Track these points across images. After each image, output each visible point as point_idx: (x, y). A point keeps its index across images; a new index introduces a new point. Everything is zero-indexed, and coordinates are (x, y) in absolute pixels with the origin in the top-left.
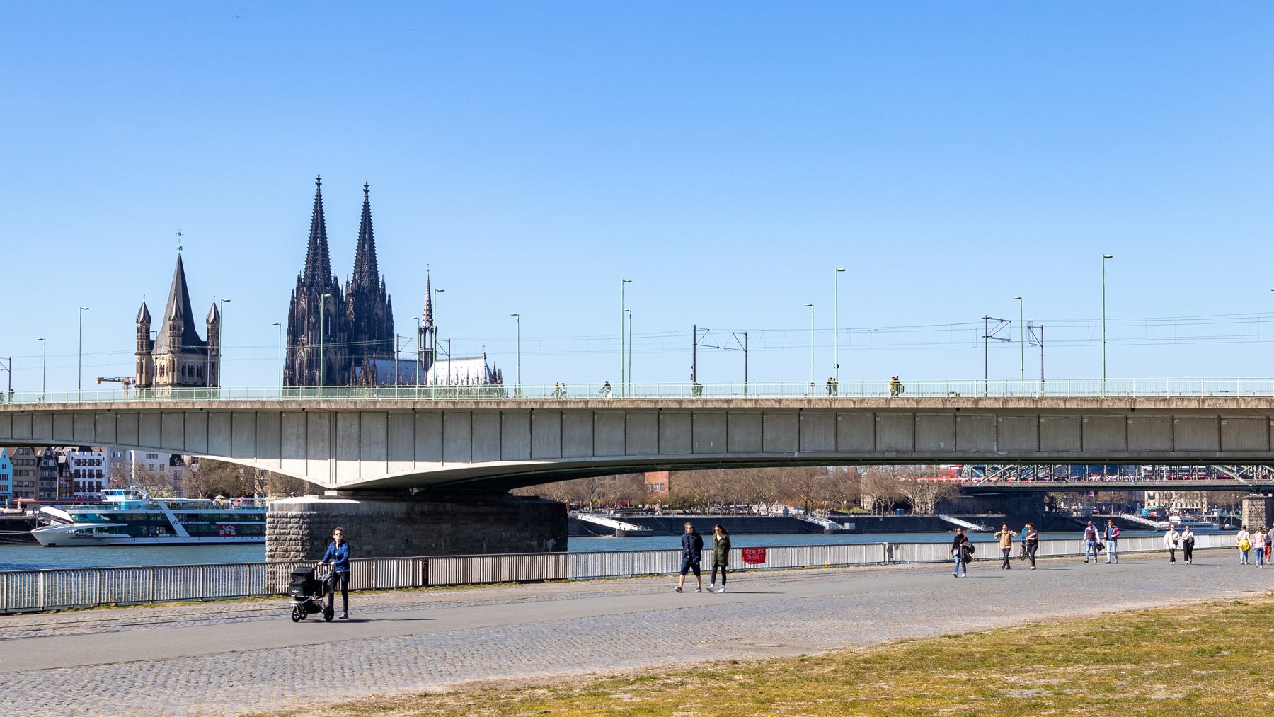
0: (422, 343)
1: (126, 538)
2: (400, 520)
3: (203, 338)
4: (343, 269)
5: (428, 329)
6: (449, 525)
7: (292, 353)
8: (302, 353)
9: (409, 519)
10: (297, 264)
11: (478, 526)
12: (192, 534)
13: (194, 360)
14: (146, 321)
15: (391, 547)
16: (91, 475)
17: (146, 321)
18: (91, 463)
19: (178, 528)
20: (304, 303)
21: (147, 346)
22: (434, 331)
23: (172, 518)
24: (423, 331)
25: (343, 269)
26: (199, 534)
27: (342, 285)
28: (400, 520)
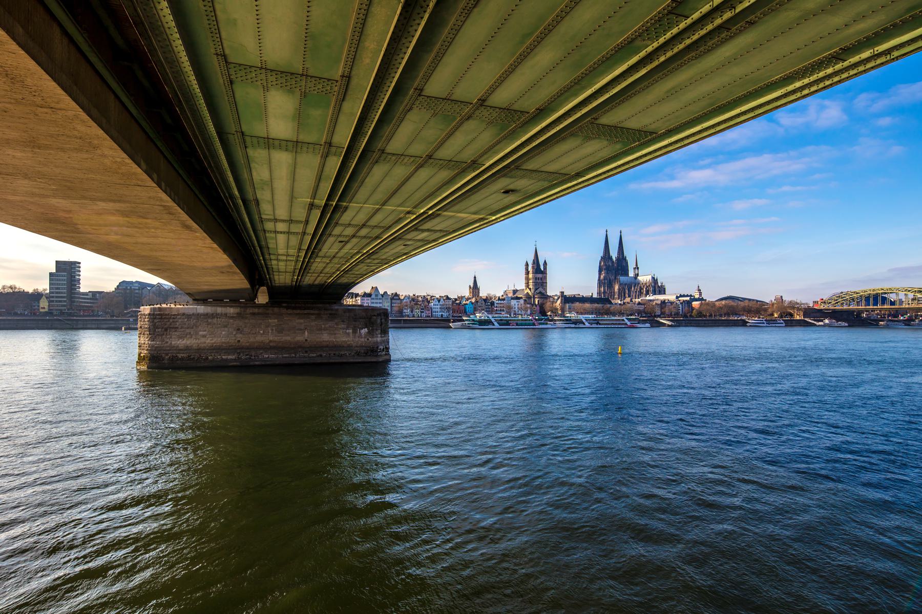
0: (634, 272)
1: (477, 326)
2: (232, 317)
3: (542, 269)
4: (614, 254)
5: (637, 268)
6: (276, 321)
7: (599, 277)
8: (602, 277)
9: (240, 316)
10: (601, 253)
11: (302, 321)
12: (500, 325)
13: (540, 276)
14: (527, 265)
15: (223, 333)
16: (501, 307)
17: (527, 265)
18: (501, 304)
19: (496, 323)
20: (602, 264)
21: (527, 273)
22: (638, 268)
23: (493, 320)
24: (635, 269)
25: (614, 254)
26: (502, 325)
27: (614, 259)
28: (232, 317)
